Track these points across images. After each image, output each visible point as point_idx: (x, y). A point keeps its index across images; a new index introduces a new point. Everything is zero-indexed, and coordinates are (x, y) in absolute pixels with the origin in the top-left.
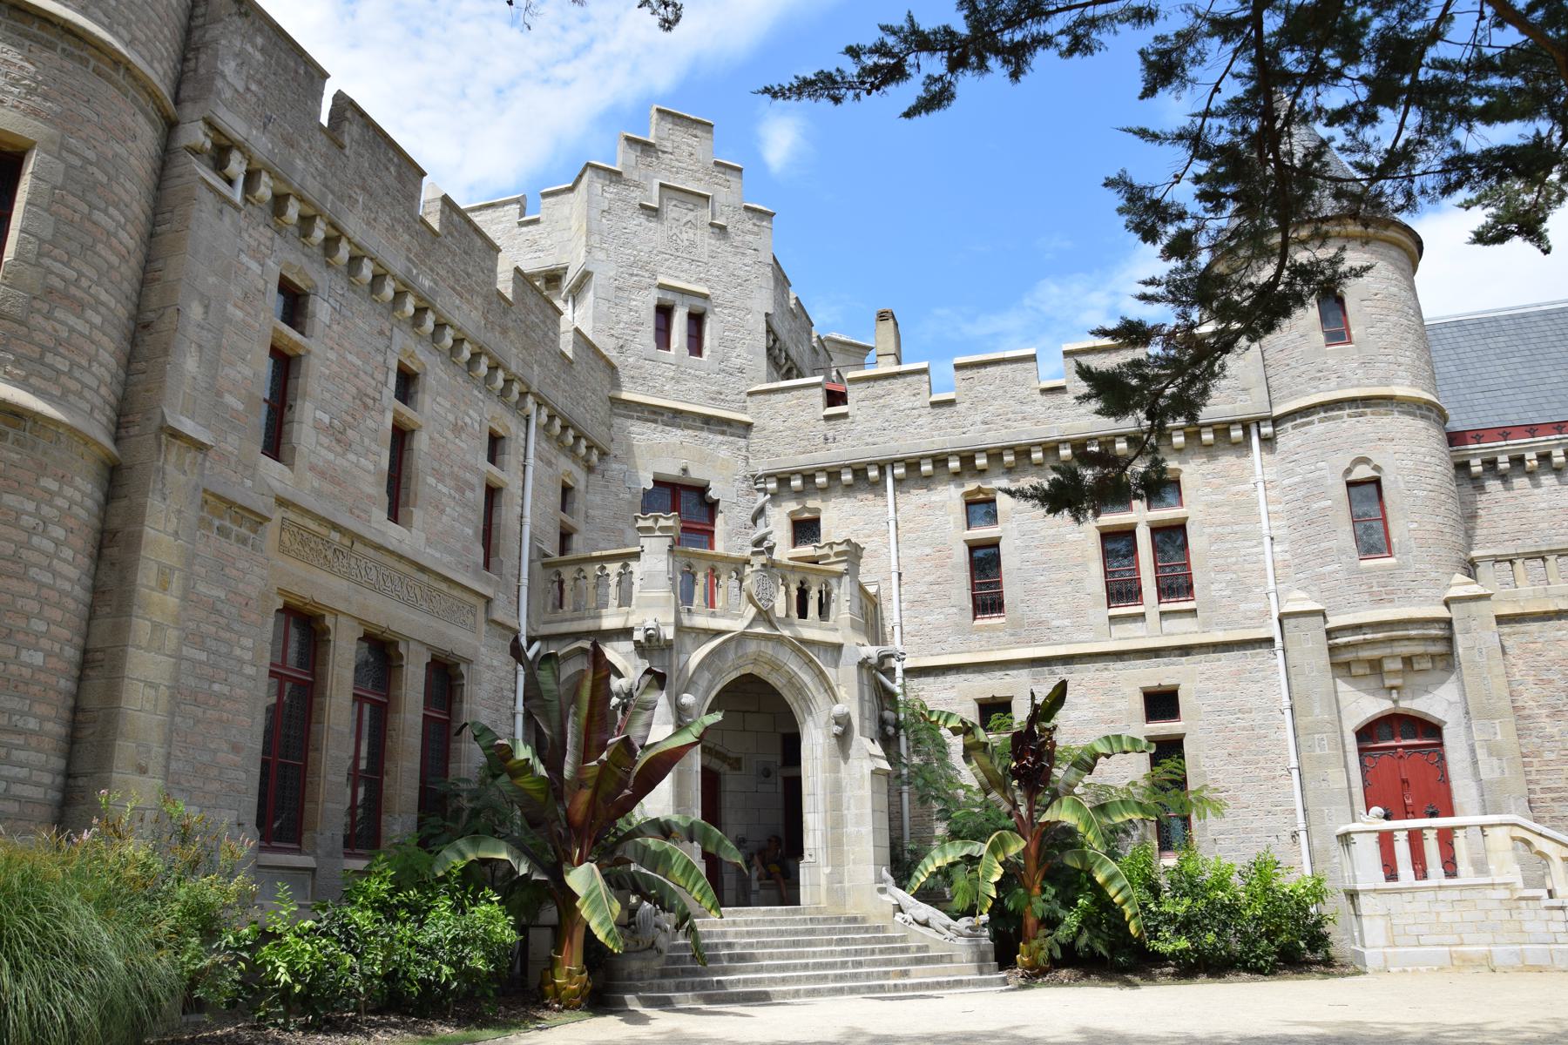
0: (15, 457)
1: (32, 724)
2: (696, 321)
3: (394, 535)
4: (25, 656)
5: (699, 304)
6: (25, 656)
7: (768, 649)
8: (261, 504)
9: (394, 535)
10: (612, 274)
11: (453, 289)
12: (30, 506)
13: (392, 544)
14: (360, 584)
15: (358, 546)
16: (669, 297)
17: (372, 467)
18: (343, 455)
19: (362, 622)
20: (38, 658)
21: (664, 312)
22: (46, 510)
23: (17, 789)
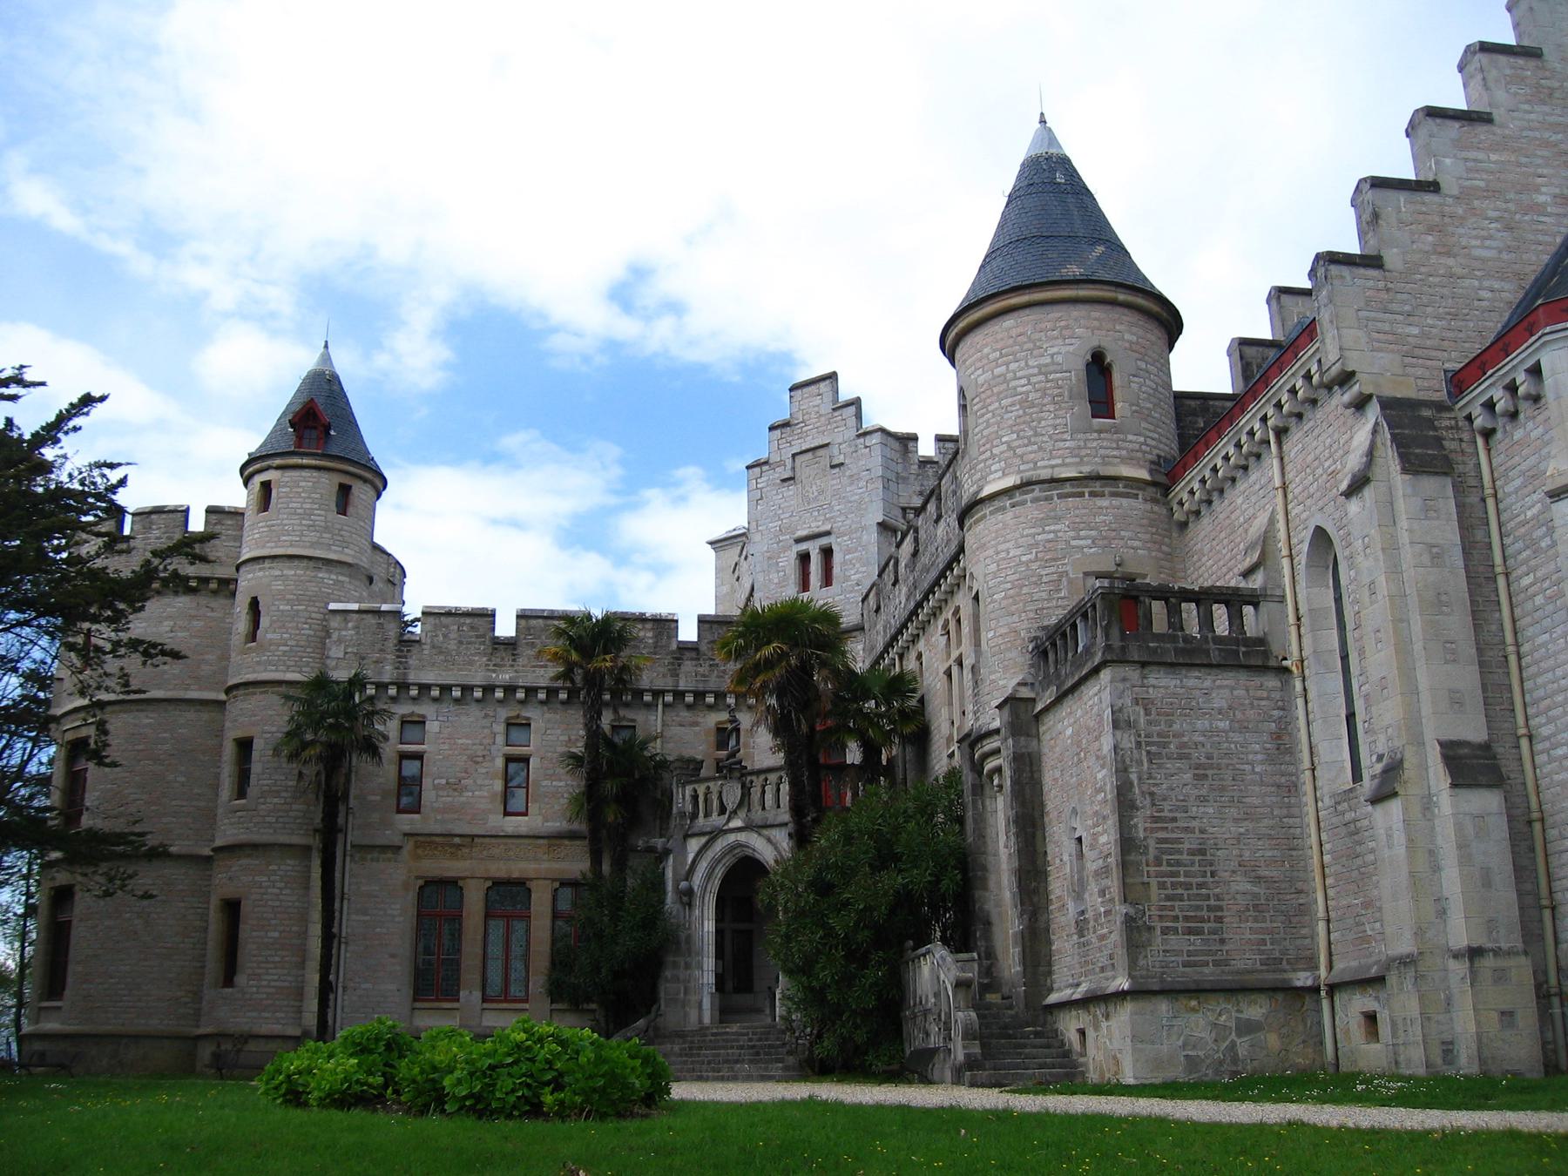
0: (257, 862)
1: (277, 959)
2: (827, 553)
3: (513, 824)
4: (270, 934)
5: (824, 541)
6: (270, 934)
7: (742, 837)
8: (397, 840)
9: (513, 824)
10: (765, 549)
11: (534, 667)
12: (265, 879)
13: (510, 830)
14: (482, 859)
15: (476, 840)
16: (803, 546)
17: (486, 794)
18: (461, 796)
19: (487, 879)
20: (276, 934)
21: (804, 558)
22: (272, 878)
23: (273, 984)
